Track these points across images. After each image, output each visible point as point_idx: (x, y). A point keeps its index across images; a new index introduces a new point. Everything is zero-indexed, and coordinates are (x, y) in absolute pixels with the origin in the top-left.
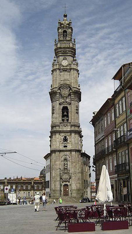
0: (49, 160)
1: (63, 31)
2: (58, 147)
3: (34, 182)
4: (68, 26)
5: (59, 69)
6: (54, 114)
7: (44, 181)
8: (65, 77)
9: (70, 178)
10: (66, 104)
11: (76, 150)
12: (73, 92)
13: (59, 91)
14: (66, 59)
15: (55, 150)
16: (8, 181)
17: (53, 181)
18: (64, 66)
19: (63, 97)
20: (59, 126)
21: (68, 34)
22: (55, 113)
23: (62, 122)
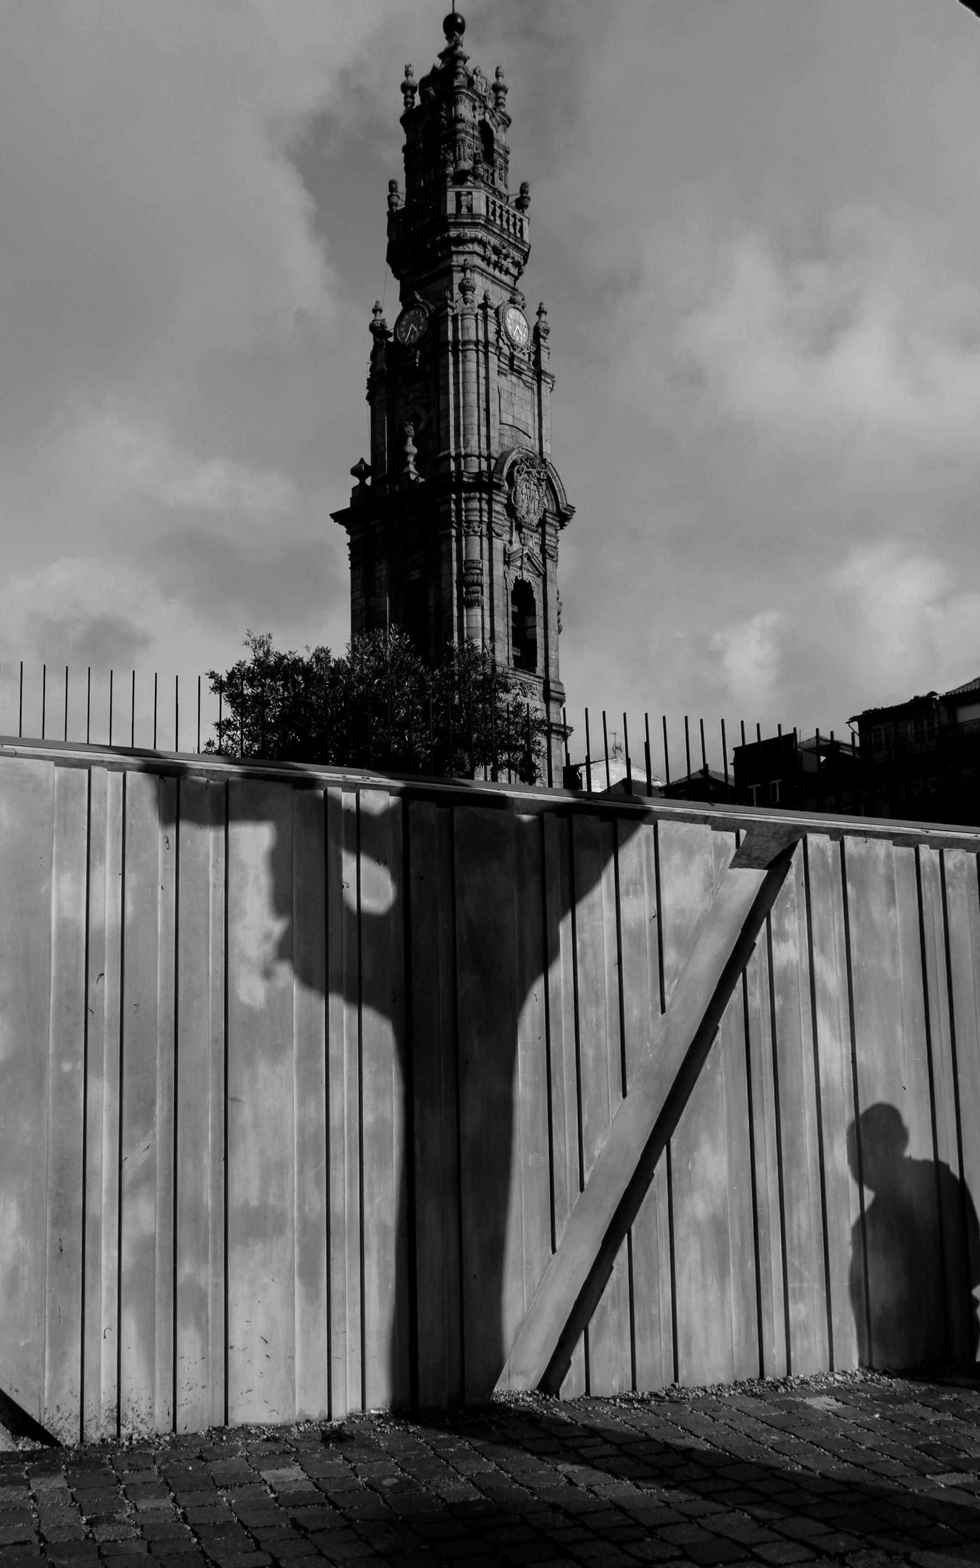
1: (480, 122)
6: (478, 611)
19: (519, 528)
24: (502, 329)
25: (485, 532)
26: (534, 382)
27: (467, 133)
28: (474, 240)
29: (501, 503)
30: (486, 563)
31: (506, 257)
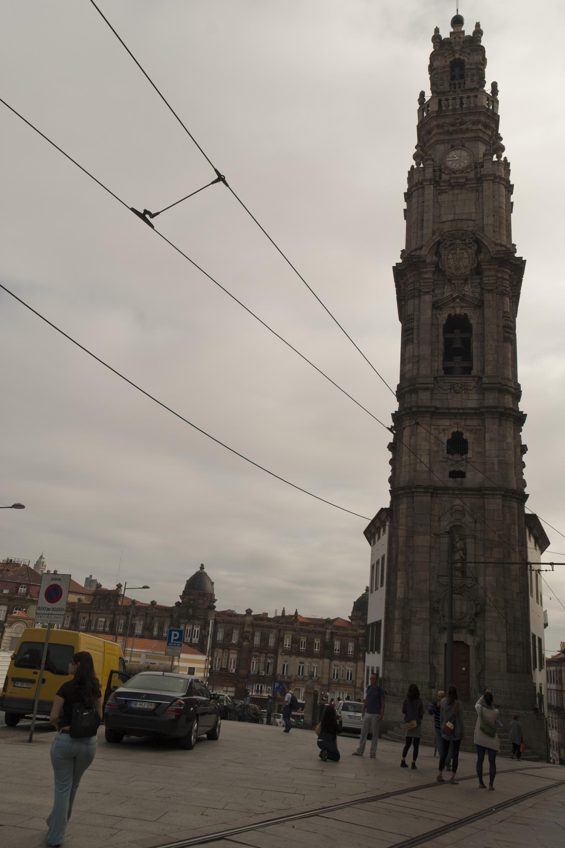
0: (384, 539)
1: (451, 62)
3: (332, 633)
5: (436, 182)
6: (410, 347)
7: (363, 631)
9: (476, 614)
10: (464, 305)
12: (493, 258)
13: (435, 258)
14: (463, 146)
16: (255, 622)
18: (454, 172)
19: (450, 280)
21: (471, 69)
22: (415, 342)
23: (442, 373)
24: (442, 167)
31: (461, 124)
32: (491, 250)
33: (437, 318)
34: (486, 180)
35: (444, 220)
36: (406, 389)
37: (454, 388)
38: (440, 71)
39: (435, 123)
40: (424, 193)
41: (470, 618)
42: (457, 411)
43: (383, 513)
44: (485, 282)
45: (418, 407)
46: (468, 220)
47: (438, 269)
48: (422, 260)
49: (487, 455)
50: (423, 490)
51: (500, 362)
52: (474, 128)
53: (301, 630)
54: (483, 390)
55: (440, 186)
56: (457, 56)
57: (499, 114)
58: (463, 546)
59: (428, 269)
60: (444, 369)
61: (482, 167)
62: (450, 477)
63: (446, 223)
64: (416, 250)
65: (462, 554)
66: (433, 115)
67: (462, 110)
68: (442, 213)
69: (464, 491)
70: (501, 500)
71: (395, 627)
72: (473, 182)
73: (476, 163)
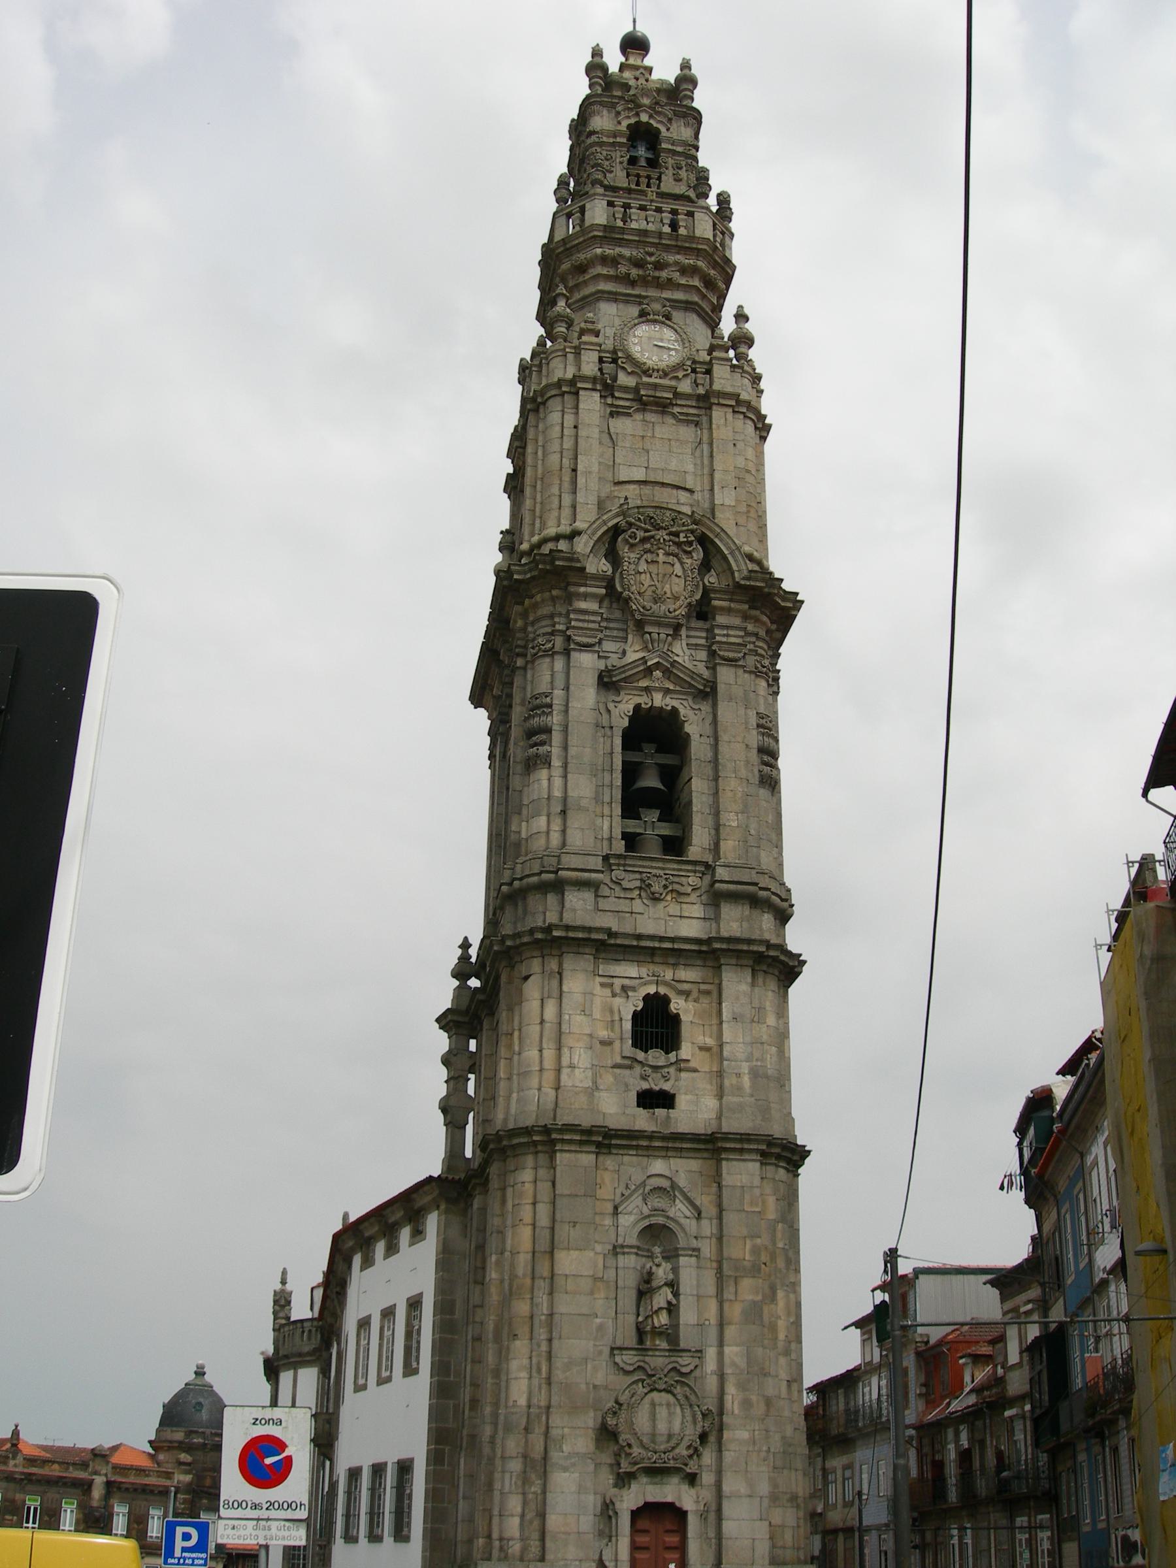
1: (629, 126)
2: (583, 1099)
3: (109, 1484)
4: (664, 100)
5: (607, 388)
6: (543, 774)
7: (188, 1478)
8: (656, 460)
9: (703, 1437)
11: (771, 1141)
12: (738, 586)
13: (605, 566)
14: (668, 317)
15: (546, 1130)
17: (515, 1466)
18: (647, 372)
19: (640, 625)
20: (594, 886)
21: (674, 153)
22: (556, 762)
23: (619, 846)
24: (620, 354)
25: (559, 641)
26: (702, 412)
27: (601, 144)
28: (590, 263)
29: (594, 596)
30: (558, 693)
31: (659, 266)
32: (735, 568)
33: (609, 711)
34: (718, 404)
35: (622, 479)
36: (535, 879)
37: (649, 885)
38: (605, 139)
39: (599, 251)
40: (577, 407)
41: (689, 1447)
42: (657, 945)
43: (426, 1188)
44: (718, 638)
45: (568, 928)
46: (678, 487)
47: (614, 596)
48: (578, 565)
49: (725, 1053)
50: (578, 1138)
51: (752, 832)
52: (683, 282)
53: (29, 1478)
54: (716, 898)
55: (613, 396)
56: (644, 118)
57: (734, 261)
58: (671, 1276)
59: (590, 590)
60: (625, 836)
61: (709, 372)
62: (638, 1106)
63: (628, 486)
64: (557, 538)
65: (670, 1296)
66: (596, 233)
67: (660, 238)
68: (618, 461)
69: (675, 1143)
70: (758, 1164)
71: (507, 1476)
72: (689, 403)
73: (694, 362)
